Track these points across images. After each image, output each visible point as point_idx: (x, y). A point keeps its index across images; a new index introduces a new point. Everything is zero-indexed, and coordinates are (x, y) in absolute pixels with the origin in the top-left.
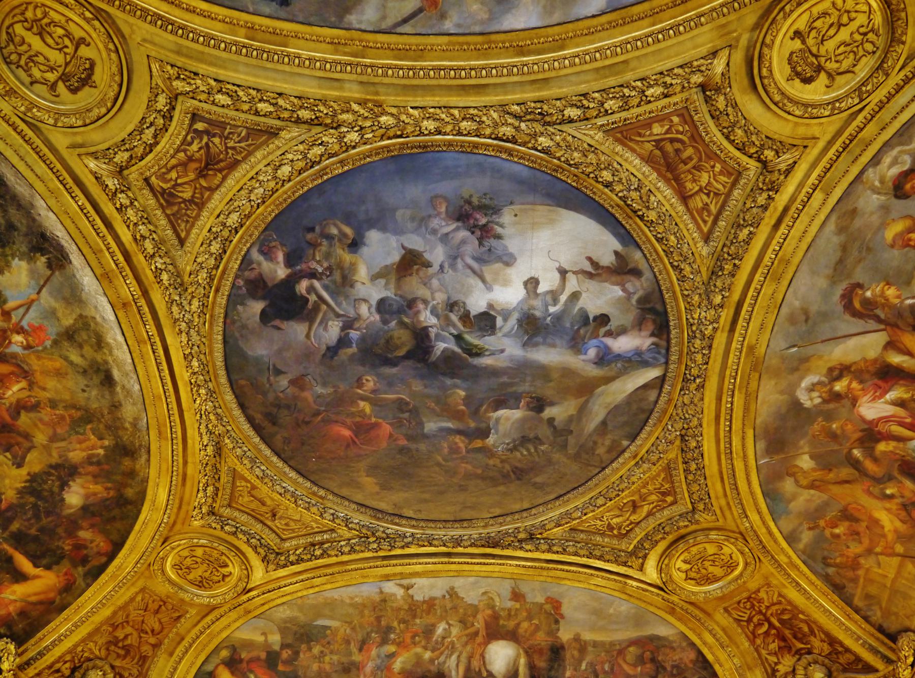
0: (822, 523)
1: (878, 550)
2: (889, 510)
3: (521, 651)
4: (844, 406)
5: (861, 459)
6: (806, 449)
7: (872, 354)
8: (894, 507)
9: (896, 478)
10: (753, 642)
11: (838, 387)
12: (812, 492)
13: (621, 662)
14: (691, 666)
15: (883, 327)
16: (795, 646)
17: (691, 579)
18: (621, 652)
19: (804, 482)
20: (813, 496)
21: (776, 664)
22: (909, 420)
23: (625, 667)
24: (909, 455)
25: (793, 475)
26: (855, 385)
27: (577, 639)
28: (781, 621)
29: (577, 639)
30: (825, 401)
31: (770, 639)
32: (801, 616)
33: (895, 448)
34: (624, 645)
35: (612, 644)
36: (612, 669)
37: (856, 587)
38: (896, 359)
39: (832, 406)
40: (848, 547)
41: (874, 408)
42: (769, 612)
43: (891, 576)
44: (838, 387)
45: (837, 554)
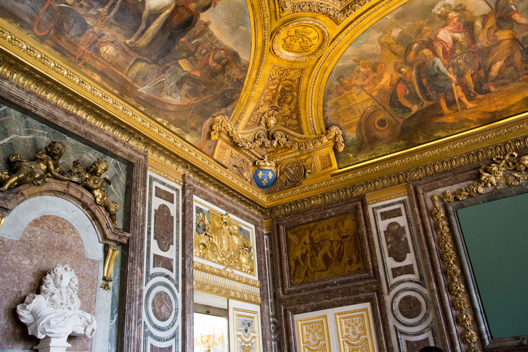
0: (361, 62)
1: (366, 88)
2: (392, 76)
3: (173, 6)
4: (440, 23)
5: (413, 49)
6: (405, 28)
7: (477, 14)
8: (396, 77)
9: (413, 67)
10: (264, 90)
11: (452, 14)
12: (379, 46)
13: (212, 54)
14: (235, 81)
15: (494, 7)
16: (274, 104)
17: (285, 41)
18: (216, 49)
19: (383, 40)
20: (376, 48)
21: (261, 106)
22: (448, 49)
23: (211, 58)
24: (429, 62)
25: (384, 32)
26: (455, 20)
27: (206, 24)
28: (283, 90)
29: (206, 24)
30: (439, 16)
31: (270, 94)
32: (295, 93)
33: (429, 55)
34: (222, 47)
35: (217, 41)
36: (205, 54)
37: (336, 97)
38: (478, 24)
39: (438, 19)
40: (357, 79)
41: (445, 35)
42: (283, 82)
43: (357, 102)
44: (452, 14)
45: (348, 79)
